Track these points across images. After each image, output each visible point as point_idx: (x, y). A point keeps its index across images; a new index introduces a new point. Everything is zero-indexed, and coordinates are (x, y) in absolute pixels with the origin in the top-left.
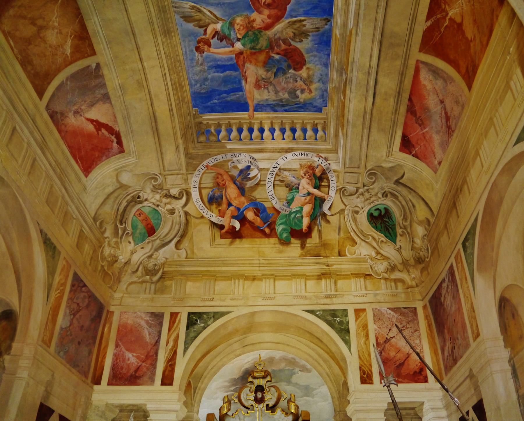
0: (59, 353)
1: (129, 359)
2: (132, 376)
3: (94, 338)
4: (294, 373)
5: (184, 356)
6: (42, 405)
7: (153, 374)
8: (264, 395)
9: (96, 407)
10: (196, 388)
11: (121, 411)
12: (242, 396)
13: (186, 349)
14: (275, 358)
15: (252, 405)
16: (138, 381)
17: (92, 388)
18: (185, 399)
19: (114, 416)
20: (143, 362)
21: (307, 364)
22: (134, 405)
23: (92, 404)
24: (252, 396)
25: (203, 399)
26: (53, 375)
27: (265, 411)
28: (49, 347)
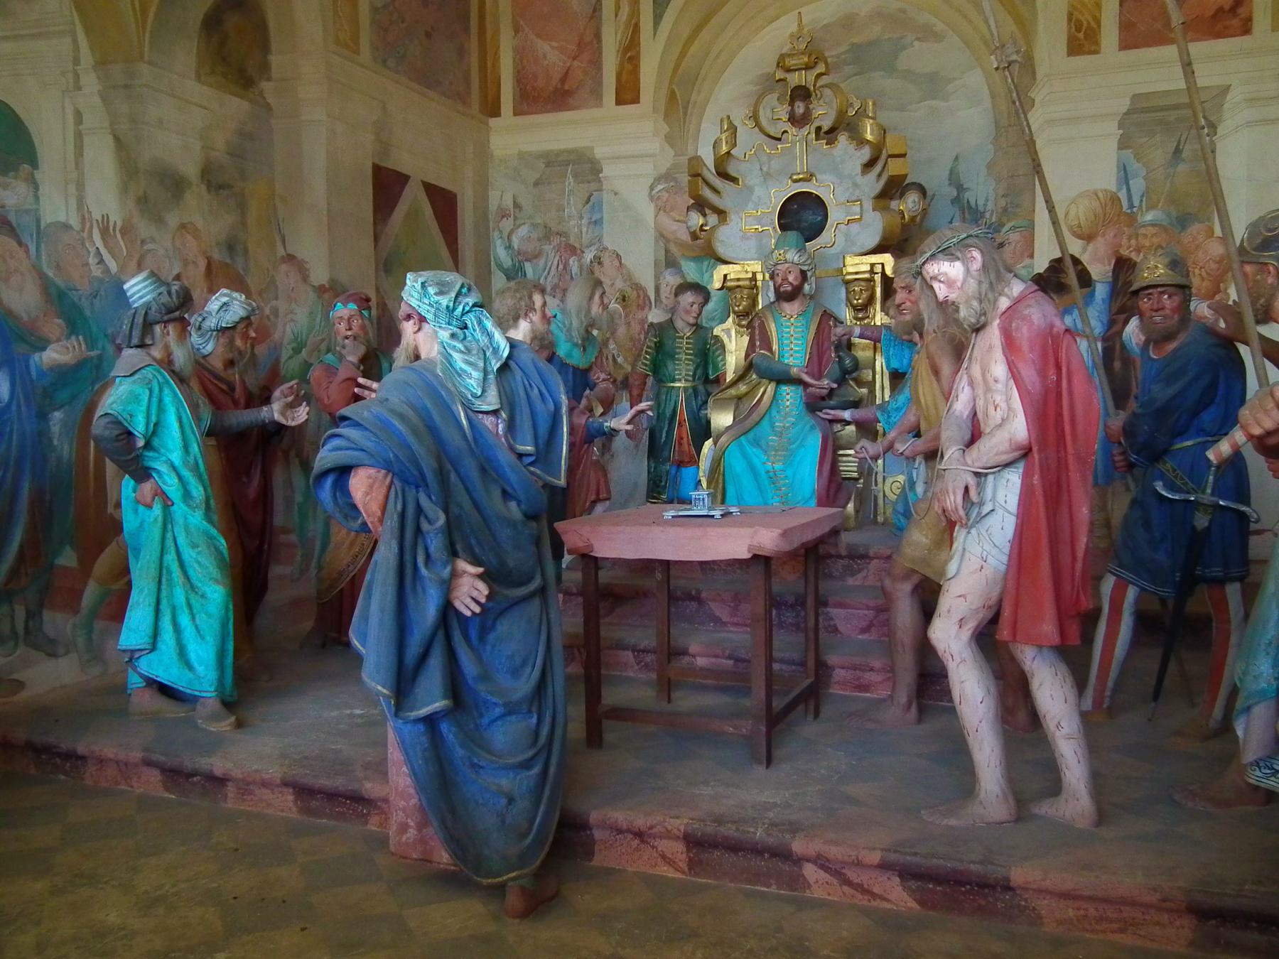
0: (384, 62)
1: (545, 56)
2: (556, 90)
3: (464, 18)
4: (904, 48)
5: (655, 34)
6: (377, 170)
7: (598, 82)
8: (811, 106)
9: (501, 160)
10: (688, 102)
11: (548, 165)
12: (761, 113)
13: (657, 19)
14: (857, 14)
15: (785, 132)
16: (571, 101)
17: (487, 124)
18: (668, 130)
19: (537, 176)
20: (574, 58)
21: (934, 20)
22: (570, 152)
23: (492, 156)
24: (783, 112)
25: (703, 125)
26: (384, 109)
27: (814, 142)
28: (357, 52)
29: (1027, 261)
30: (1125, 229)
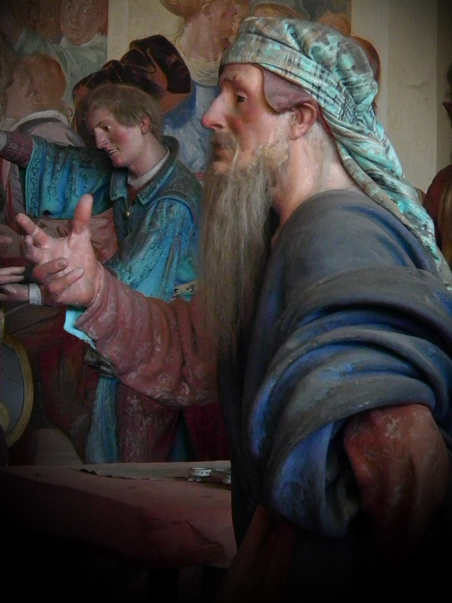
29: (97, 39)
30: (237, 7)
